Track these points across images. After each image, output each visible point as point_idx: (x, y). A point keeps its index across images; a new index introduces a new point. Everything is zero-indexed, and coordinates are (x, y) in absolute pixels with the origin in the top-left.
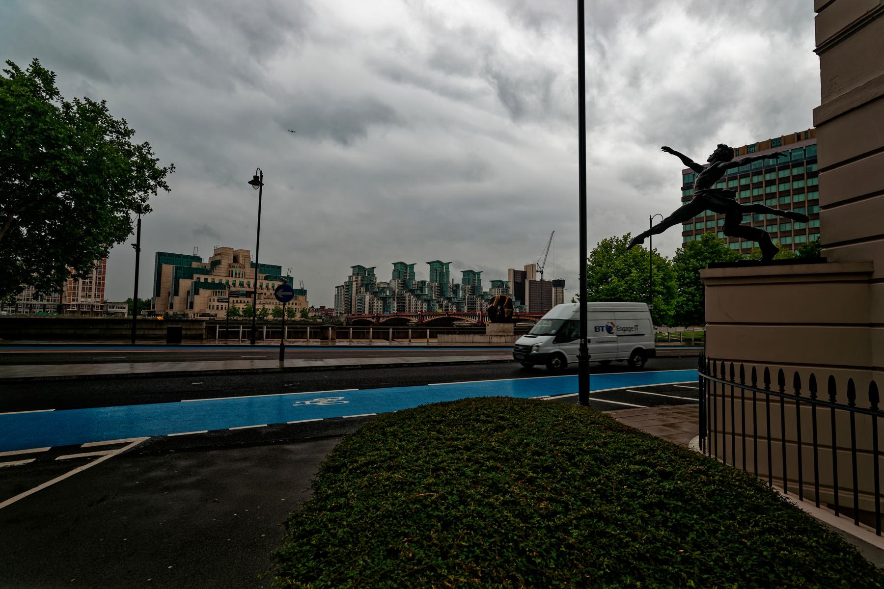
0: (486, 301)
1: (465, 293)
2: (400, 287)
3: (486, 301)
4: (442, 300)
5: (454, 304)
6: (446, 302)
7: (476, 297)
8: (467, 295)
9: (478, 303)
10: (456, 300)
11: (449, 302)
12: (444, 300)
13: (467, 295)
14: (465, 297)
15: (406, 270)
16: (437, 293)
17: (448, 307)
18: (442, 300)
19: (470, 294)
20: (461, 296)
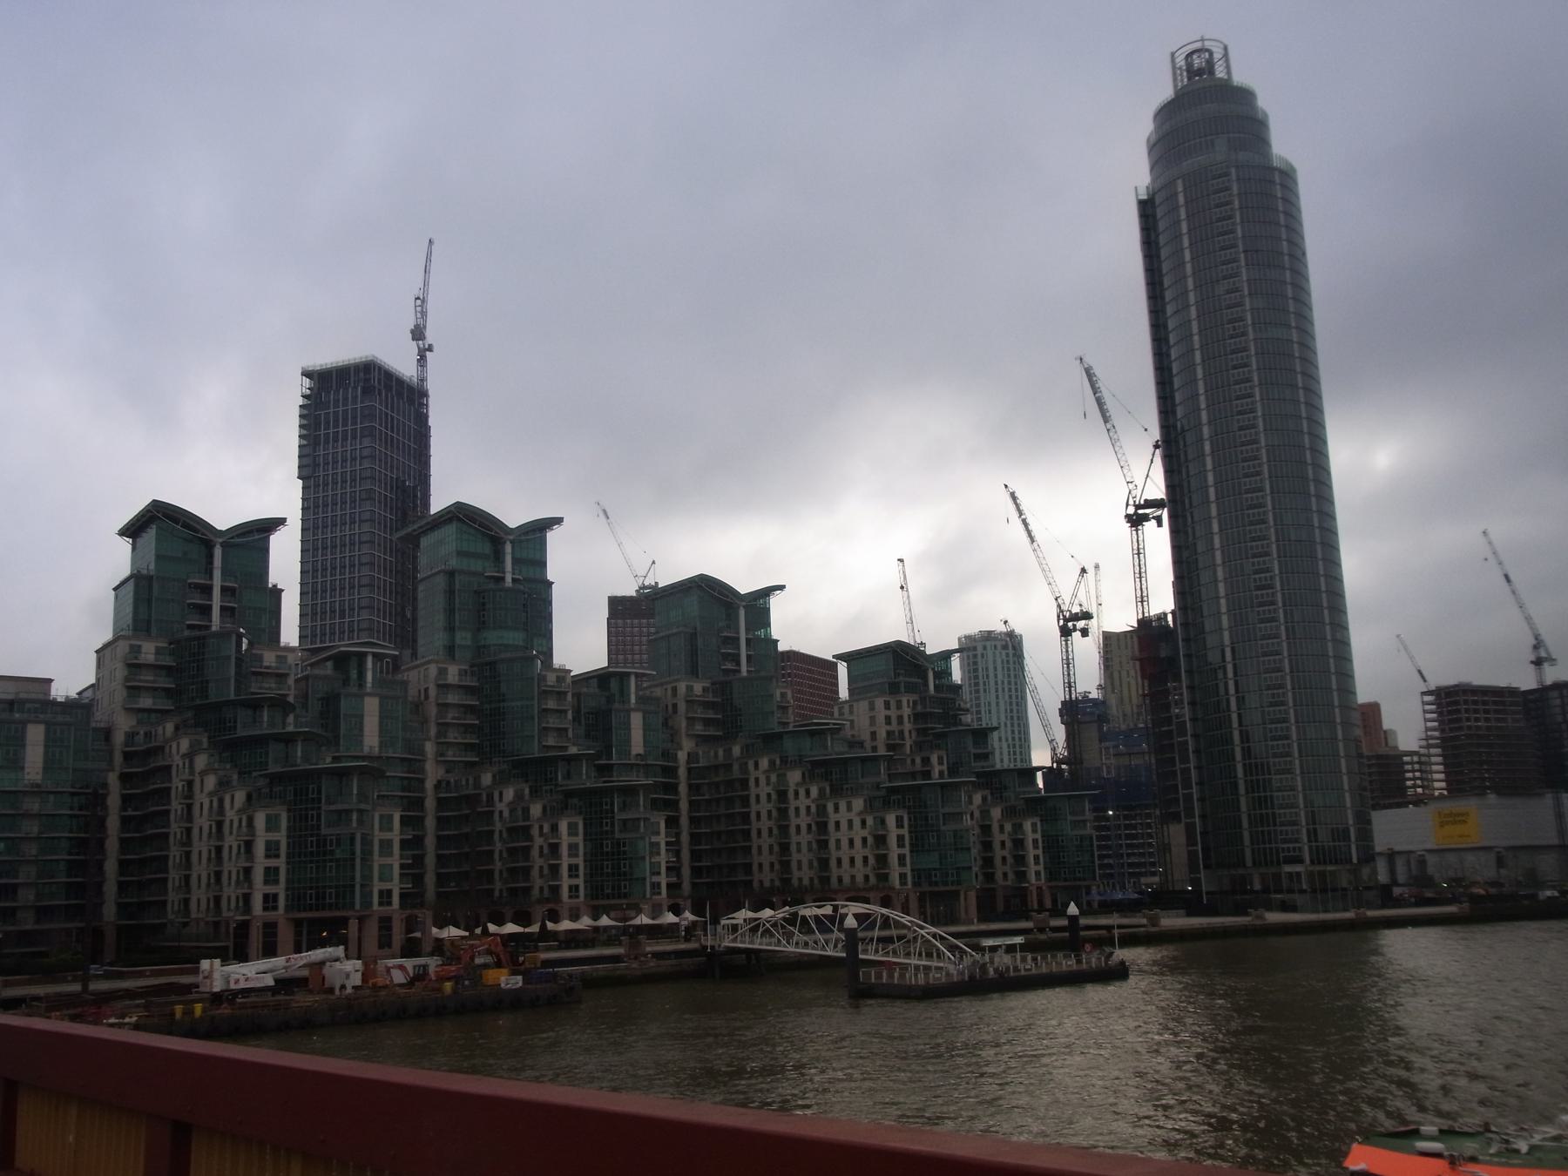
0: (808, 777)
1: (673, 736)
2: (146, 702)
3: (808, 777)
4: (487, 779)
5: (566, 801)
6: (509, 794)
7: (748, 750)
8: (687, 745)
9: (761, 789)
10: (586, 779)
11: (535, 792)
12: (501, 780)
13: (687, 745)
14: (668, 755)
15: (209, 573)
16: (453, 736)
17: (526, 830)
18: (487, 779)
19: (703, 740)
20: (637, 745)
